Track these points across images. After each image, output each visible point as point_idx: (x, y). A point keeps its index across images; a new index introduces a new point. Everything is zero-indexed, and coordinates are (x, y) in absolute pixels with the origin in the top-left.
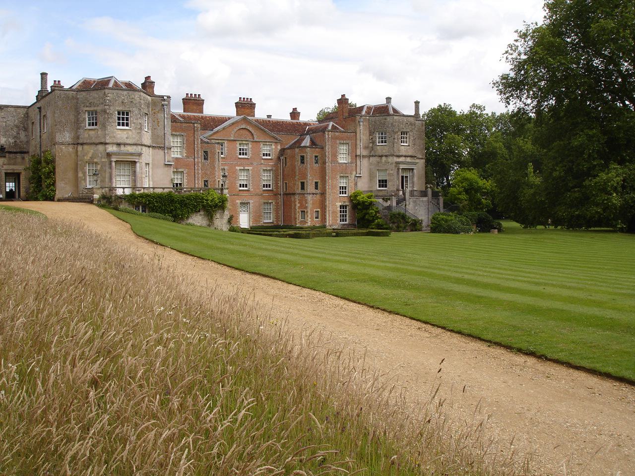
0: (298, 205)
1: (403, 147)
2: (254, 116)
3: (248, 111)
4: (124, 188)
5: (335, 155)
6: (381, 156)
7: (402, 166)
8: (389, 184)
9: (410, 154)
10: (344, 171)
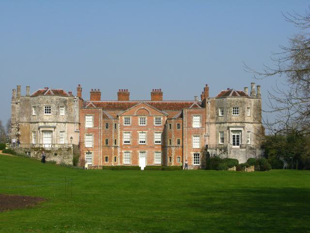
0: (168, 153)
1: (234, 117)
2: (161, 100)
3: (158, 97)
4: (49, 144)
5: (190, 123)
6: (221, 123)
7: (231, 129)
8: (225, 140)
9: (240, 121)
10: (197, 133)
